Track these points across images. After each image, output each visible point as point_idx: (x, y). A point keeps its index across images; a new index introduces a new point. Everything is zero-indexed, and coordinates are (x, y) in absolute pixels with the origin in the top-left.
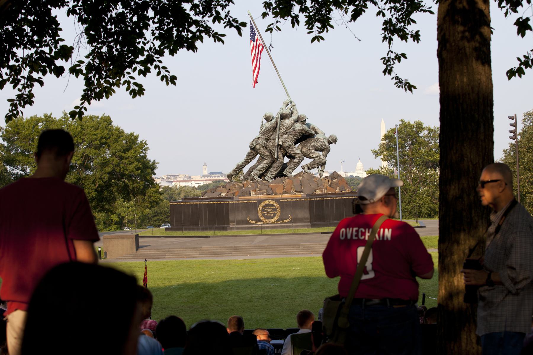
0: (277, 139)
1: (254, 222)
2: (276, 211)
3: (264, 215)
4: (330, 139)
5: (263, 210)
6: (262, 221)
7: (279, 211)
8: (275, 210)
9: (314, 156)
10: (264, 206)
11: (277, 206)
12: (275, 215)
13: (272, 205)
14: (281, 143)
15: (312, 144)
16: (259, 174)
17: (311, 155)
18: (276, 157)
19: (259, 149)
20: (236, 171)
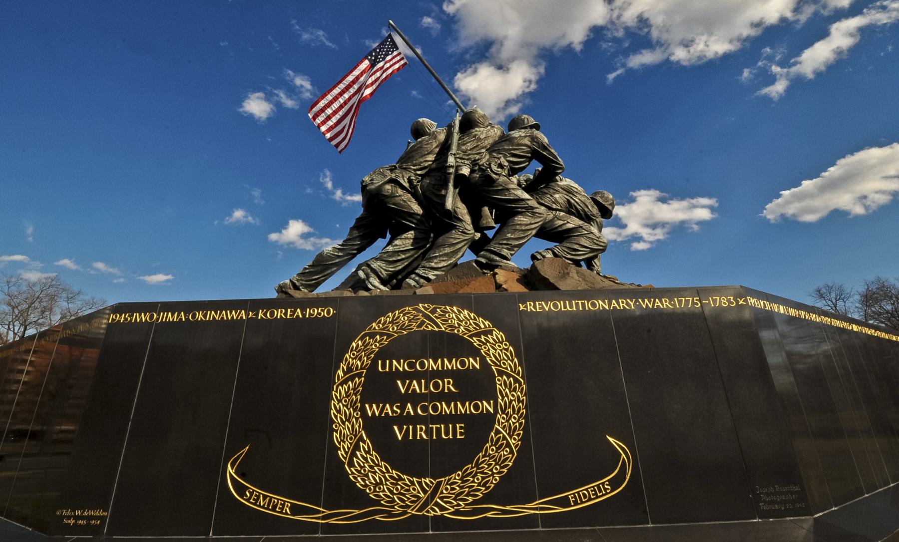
0: (451, 160)
1: (282, 506)
2: (491, 395)
3: (378, 430)
4: (598, 198)
5: (378, 386)
6: (358, 498)
7: (511, 396)
8: (477, 384)
9: (570, 226)
10: (384, 354)
11: (497, 349)
12: (479, 428)
13: (453, 344)
14: (466, 171)
15: (557, 196)
16: (384, 274)
17: (561, 222)
18: (449, 204)
19: (392, 196)
20: (311, 274)
